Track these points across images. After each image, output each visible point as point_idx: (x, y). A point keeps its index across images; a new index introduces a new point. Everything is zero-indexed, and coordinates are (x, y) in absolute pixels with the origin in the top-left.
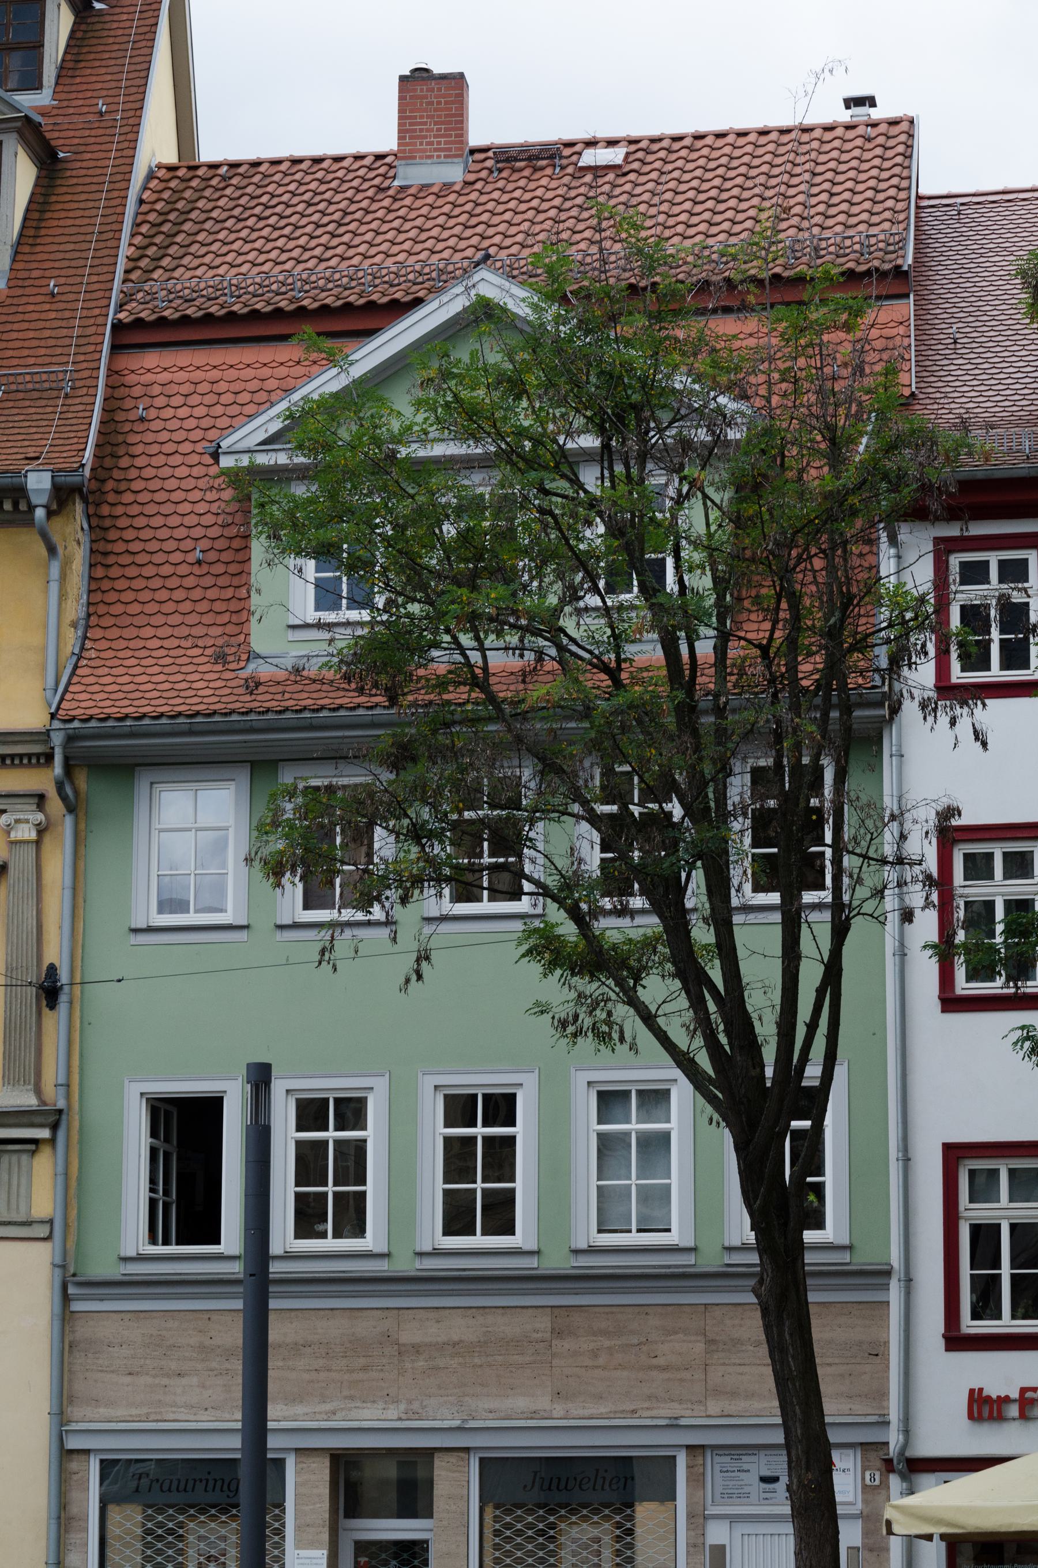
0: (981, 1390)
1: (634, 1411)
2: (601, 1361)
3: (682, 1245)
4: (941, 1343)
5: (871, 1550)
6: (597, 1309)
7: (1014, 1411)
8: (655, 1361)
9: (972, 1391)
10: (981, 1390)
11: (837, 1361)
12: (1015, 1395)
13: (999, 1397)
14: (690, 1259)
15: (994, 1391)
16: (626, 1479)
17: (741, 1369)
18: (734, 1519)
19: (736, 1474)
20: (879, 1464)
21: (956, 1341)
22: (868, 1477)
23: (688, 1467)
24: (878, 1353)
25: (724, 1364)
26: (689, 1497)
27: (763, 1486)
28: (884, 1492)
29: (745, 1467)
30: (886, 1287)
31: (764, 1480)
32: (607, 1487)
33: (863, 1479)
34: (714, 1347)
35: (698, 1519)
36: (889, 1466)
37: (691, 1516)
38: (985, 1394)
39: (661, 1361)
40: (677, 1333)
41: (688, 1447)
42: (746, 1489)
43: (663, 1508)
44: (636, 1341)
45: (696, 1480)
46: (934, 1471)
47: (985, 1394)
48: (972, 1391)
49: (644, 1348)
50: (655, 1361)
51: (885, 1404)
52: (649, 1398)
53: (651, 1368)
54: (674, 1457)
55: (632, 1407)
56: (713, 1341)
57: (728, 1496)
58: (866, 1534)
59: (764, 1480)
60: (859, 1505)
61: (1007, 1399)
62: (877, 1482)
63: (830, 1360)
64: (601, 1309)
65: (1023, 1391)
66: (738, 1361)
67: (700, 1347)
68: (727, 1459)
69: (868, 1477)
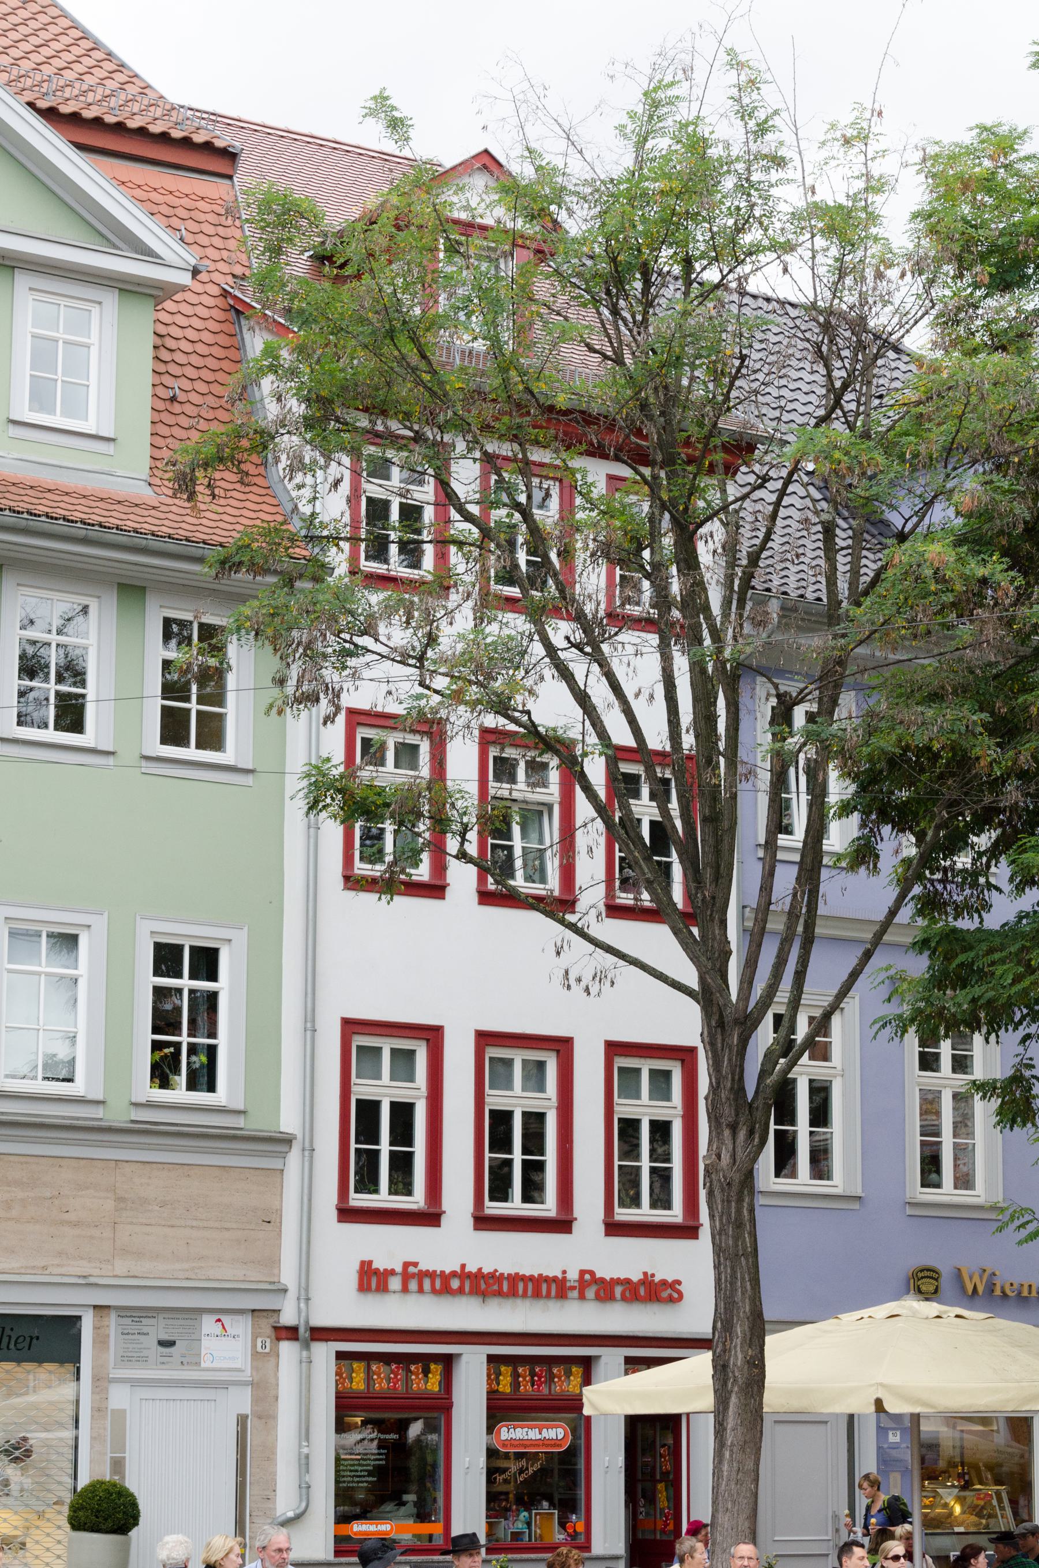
0: (370, 1262)
1: (45, 1268)
2: (14, 1213)
3: (90, 1097)
4: (334, 1214)
5: (260, 1418)
6: (12, 1158)
7: (395, 1283)
8: (66, 1216)
9: (363, 1263)
10: (370, 1262)
11: (234, 1226)
12: (399, 1269)
13: (385, 1270)
14: (98, 1112)
15: (379, 1264)
16: (32, 1338)
17: (148, 1229)
18: (135, 1383)
19: (136, 1337)
20: (269, 1331)
21: (347, 1214)
22: (259, 1344)
23: (95, 1328)
24: (271, 1220)
25: (132, 1223)
26: (95, 1358)
27: (161, 1349)
28: (273, 1360)
29: (145, 1330)
30: (284, 1156)
31: (162, 1343)
32: (12, 1346)
33: (254, 1346)
34: (122, 1205)
35: (101, 1381)
36: (291, 1333)
37: (96, 1379)
38: (374, 1266)
39: (72, 1217)
40: (87, 1188)
41: (95, 1307)
42: (145, 1353)
43: (62, 1370)
44: (48, 1195)
45: (101, 1341)
46: (327, 1340)
47: (374, 1266)
48: (363, 1263)
49: (56, 1202)
50: (66, 1216)
51: (276, 1271)
52: (60, 1254)
53: (63, 1223)
54: (79, 1318)
55: (43, 1264)
56: (120, 1199)
57: (126, 1359)
58: (256, 1401)
59: (162, 1343)
60: (249, 1372)
61: (393, 1272)
62: (267, 1350)
63: (228, 1225)
64: (16, 1158)
65: (406, 1265)
66: (144, 1221)
67: (109, 1205)
68: (128, 1321)
69: (259, 1344)
